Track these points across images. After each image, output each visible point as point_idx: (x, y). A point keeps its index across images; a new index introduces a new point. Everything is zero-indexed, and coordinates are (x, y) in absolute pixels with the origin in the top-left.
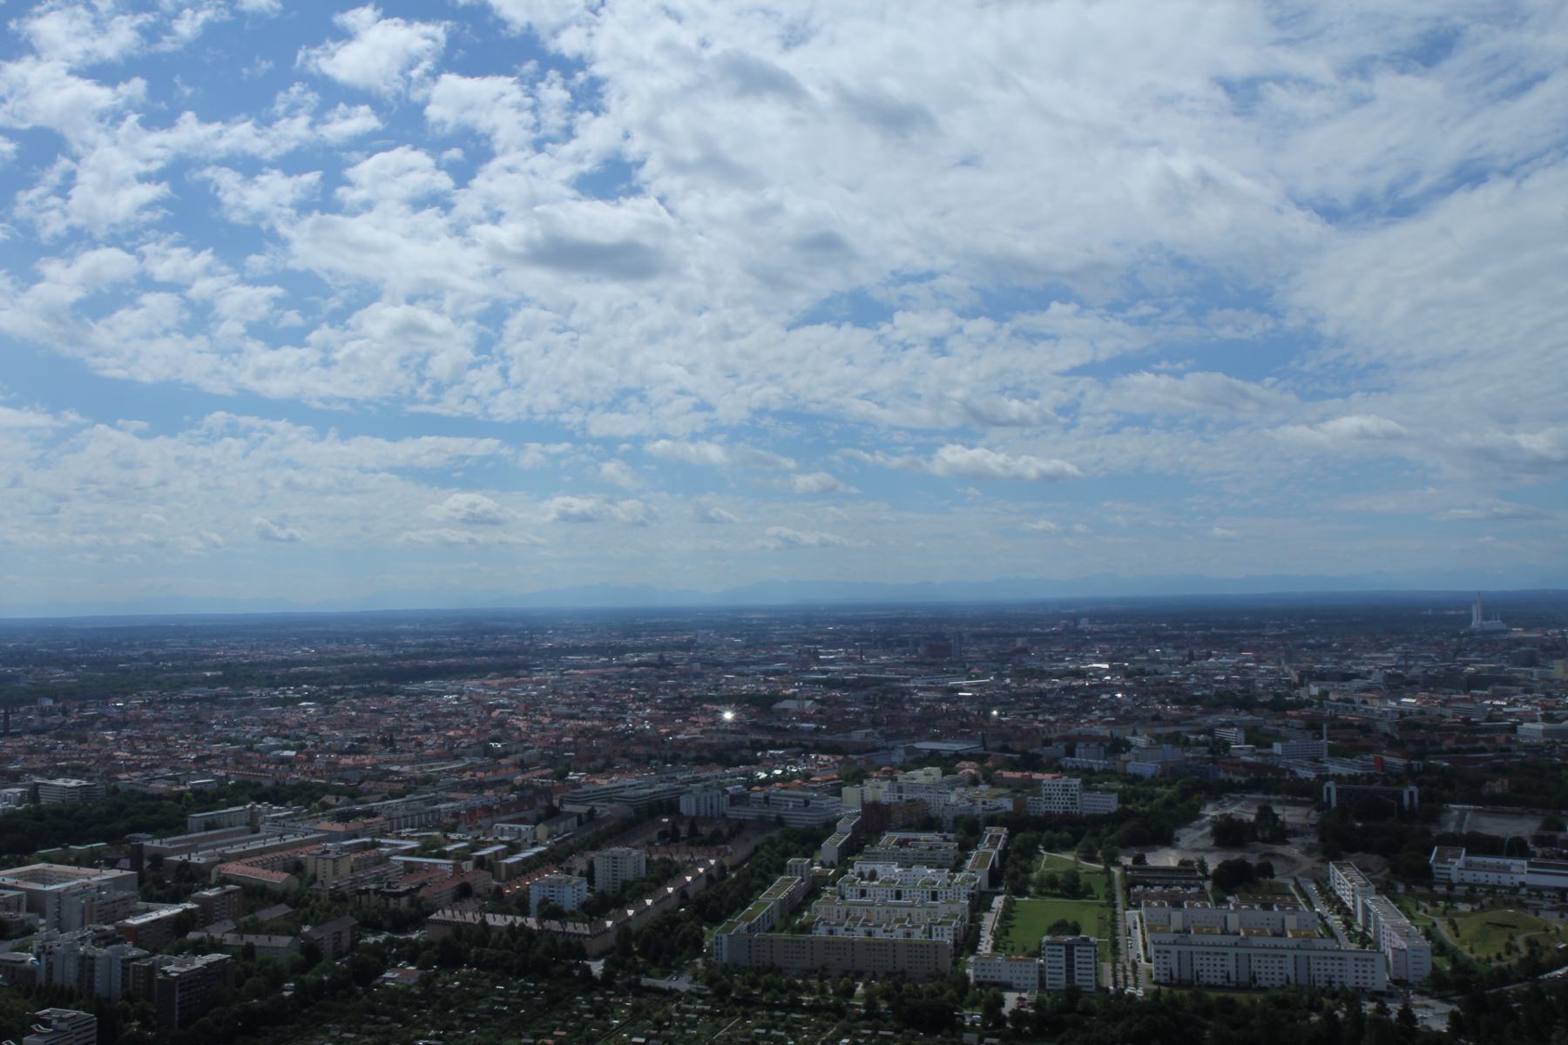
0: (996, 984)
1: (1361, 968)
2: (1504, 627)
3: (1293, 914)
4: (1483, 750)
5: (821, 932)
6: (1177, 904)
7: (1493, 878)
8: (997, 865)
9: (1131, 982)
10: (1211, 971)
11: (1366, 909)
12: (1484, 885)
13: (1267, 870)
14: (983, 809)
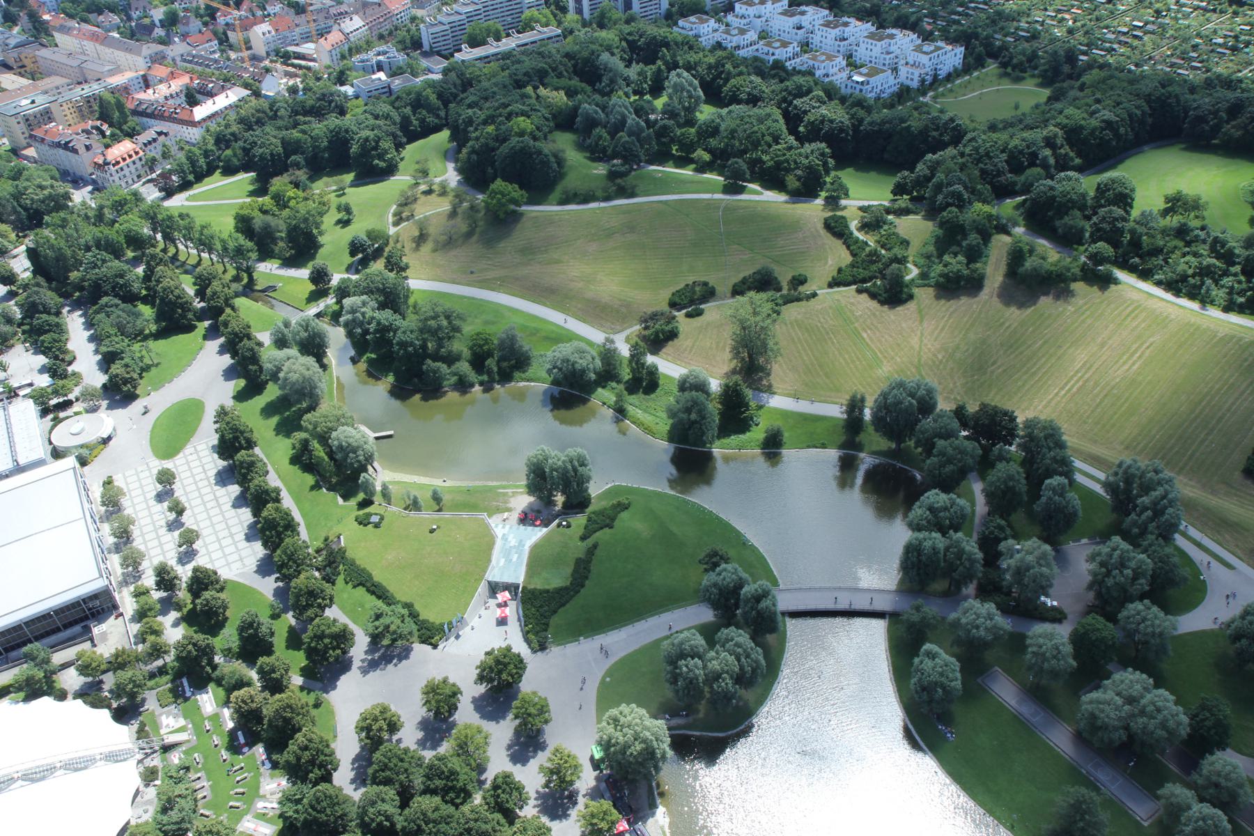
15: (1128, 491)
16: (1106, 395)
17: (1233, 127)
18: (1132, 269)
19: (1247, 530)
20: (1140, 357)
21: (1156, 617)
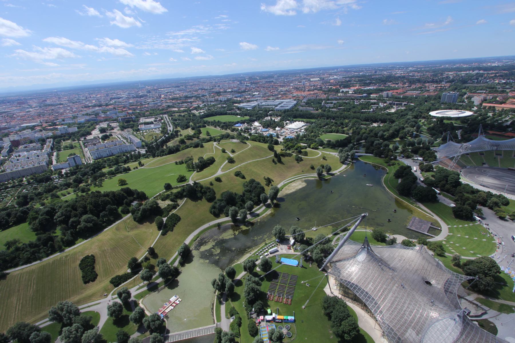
0: (59, 169)
5: (9, 171)
6: (95, 145)
7: (149, 128)
8: (52, 146)
9: (89, 160)
10: (104, 155)
11: (130, 138)
13: (111, 135)
15: (59, 315)
16: (32, 301)
17: (12, 218)
18: (11, 267)
19: (96, 293)
20: (34, 284)
21: (91, 333)
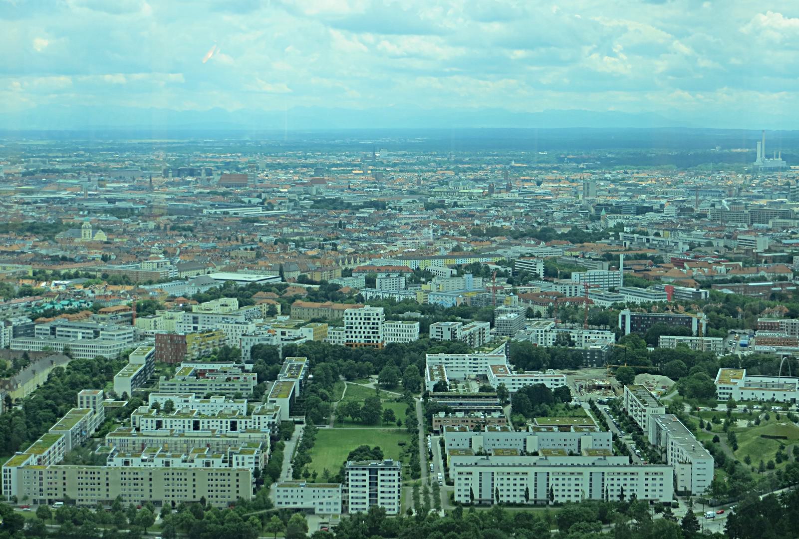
1: (650, 482)
2: (784, 164)
3: (589, 434)
4: (763, 279)
6: (478, 428)
8: (297, 394)
11: (658, 428)
12: (760, 403)
14: (282, 339)
